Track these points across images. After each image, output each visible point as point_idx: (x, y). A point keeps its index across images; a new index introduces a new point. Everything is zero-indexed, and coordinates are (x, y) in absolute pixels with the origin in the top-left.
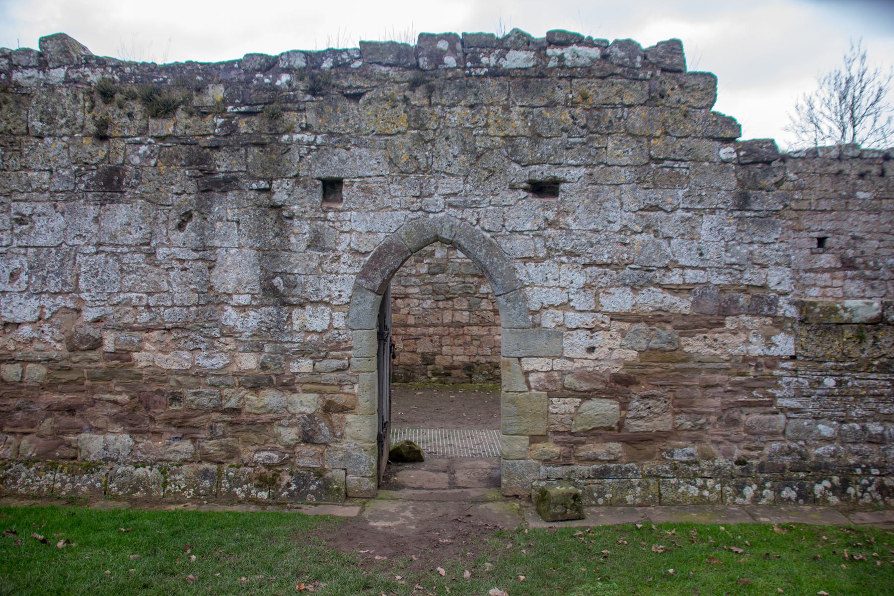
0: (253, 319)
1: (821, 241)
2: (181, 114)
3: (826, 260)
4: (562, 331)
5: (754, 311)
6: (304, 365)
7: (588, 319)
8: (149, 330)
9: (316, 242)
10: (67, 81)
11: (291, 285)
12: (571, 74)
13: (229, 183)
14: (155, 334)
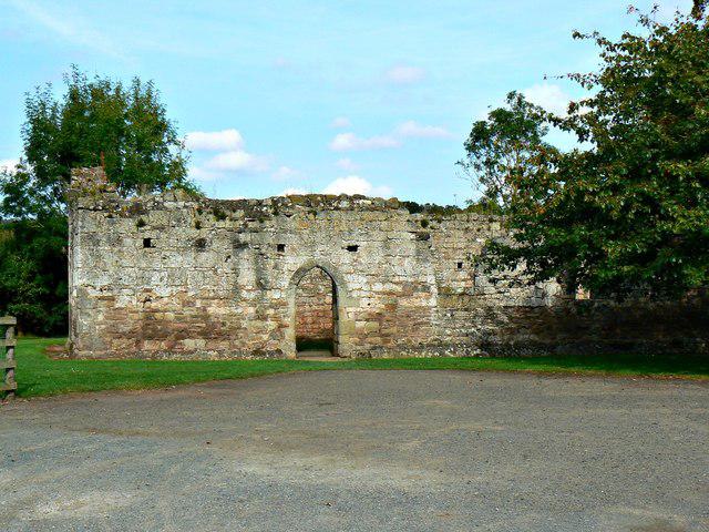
0: (253, 295)
1: (460, 265)
2: (227, 221)
3: (462, 275)
4: (360, 298)
5: (424, 290)
6: (271, 312)
7: (368, 294)
8: (214, 299)
9: (276, 267)
10: (185, 207)
11: (267, 282)
12: (362, 209)
13: (244, 245)
14: (216, 301)
